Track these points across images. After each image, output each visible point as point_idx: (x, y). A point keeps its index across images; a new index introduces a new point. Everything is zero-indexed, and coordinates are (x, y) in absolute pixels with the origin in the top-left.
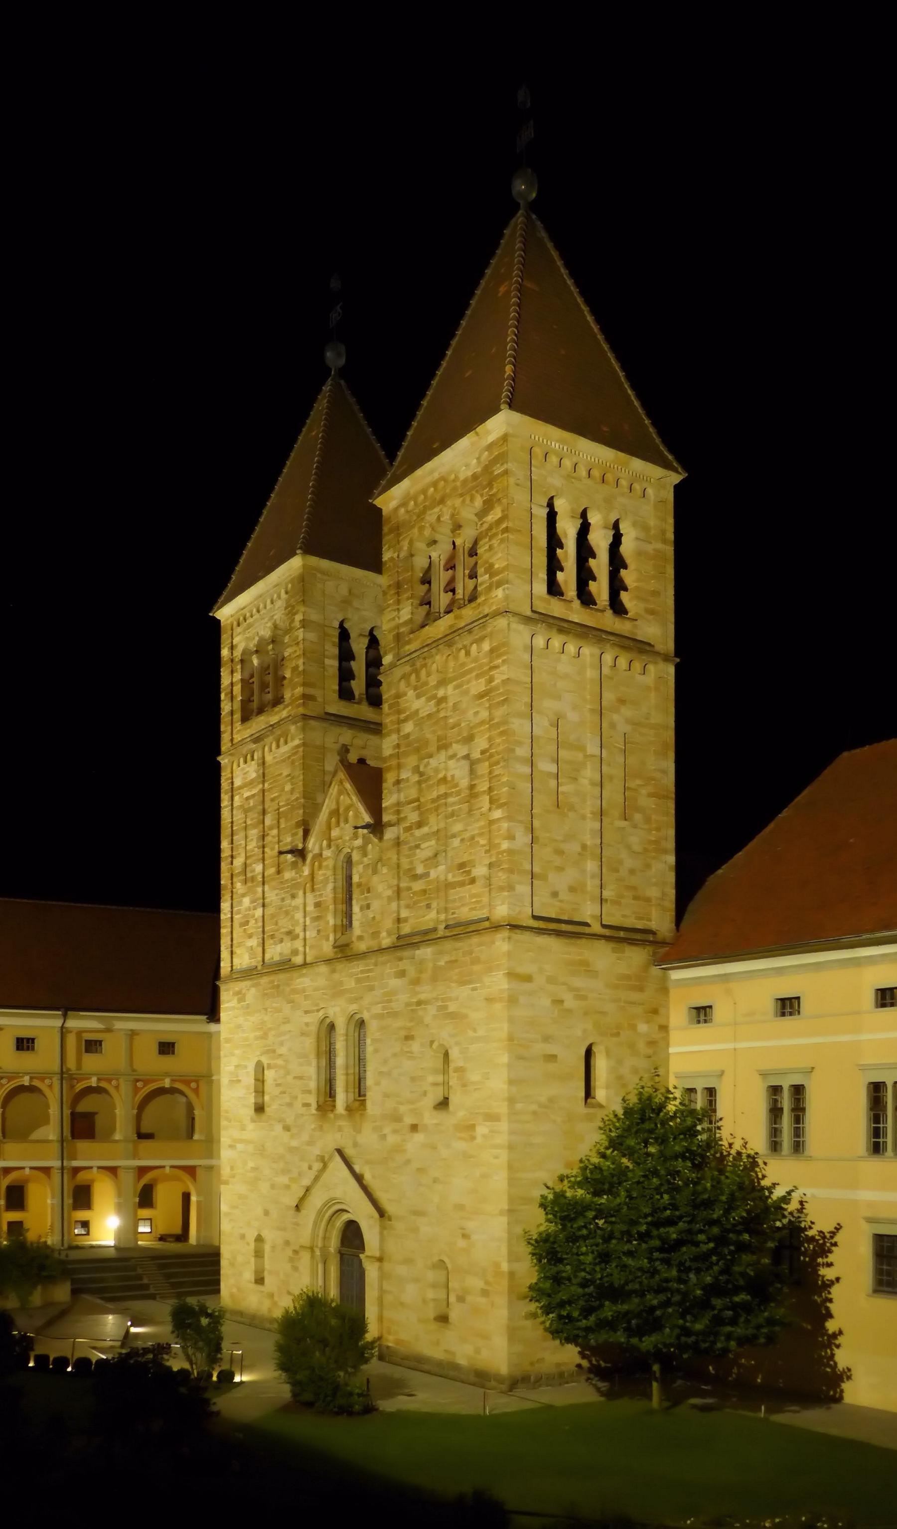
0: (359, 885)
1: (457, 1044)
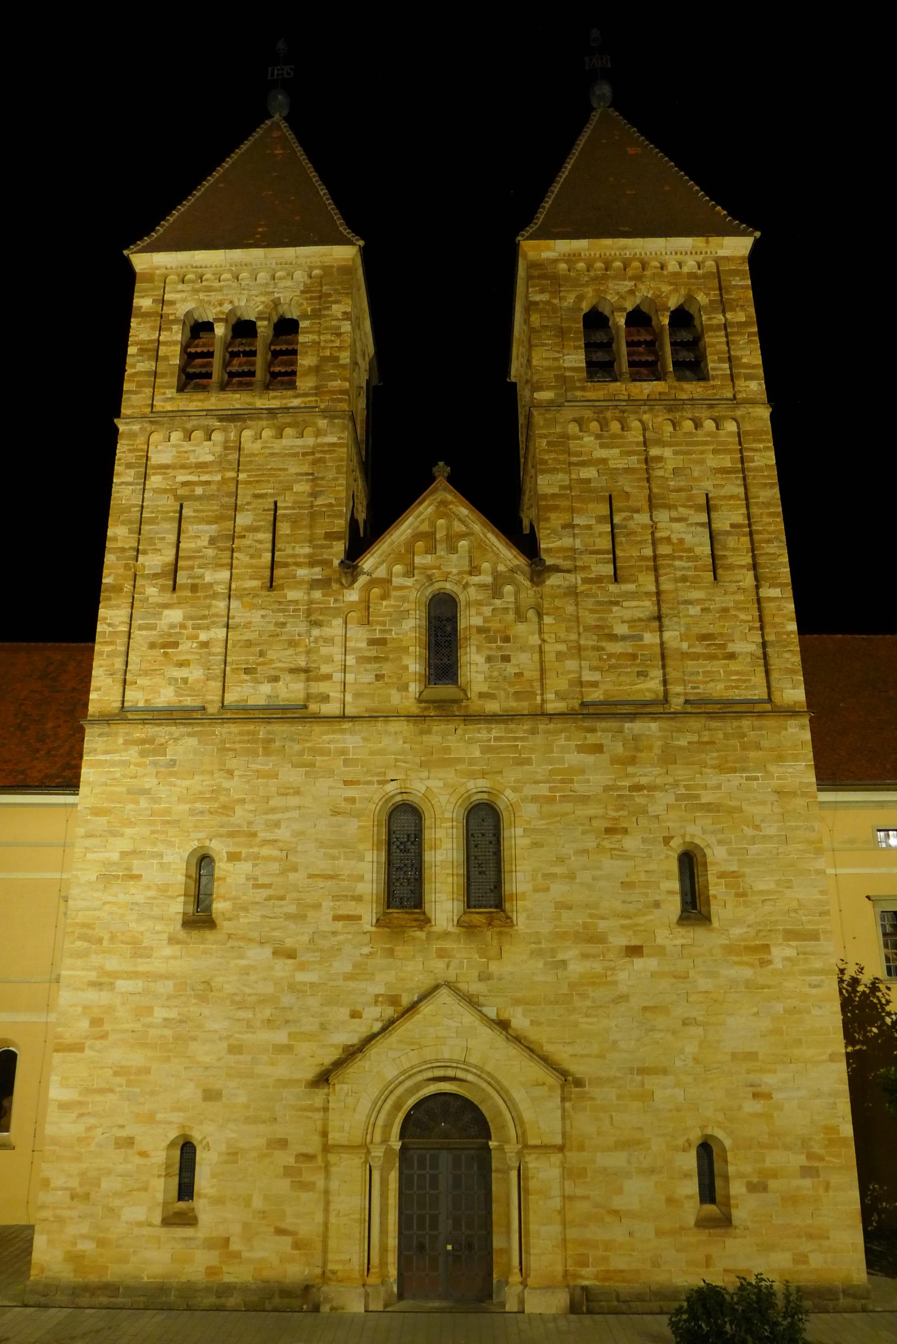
0: (480, 630)
1: (720, 842)
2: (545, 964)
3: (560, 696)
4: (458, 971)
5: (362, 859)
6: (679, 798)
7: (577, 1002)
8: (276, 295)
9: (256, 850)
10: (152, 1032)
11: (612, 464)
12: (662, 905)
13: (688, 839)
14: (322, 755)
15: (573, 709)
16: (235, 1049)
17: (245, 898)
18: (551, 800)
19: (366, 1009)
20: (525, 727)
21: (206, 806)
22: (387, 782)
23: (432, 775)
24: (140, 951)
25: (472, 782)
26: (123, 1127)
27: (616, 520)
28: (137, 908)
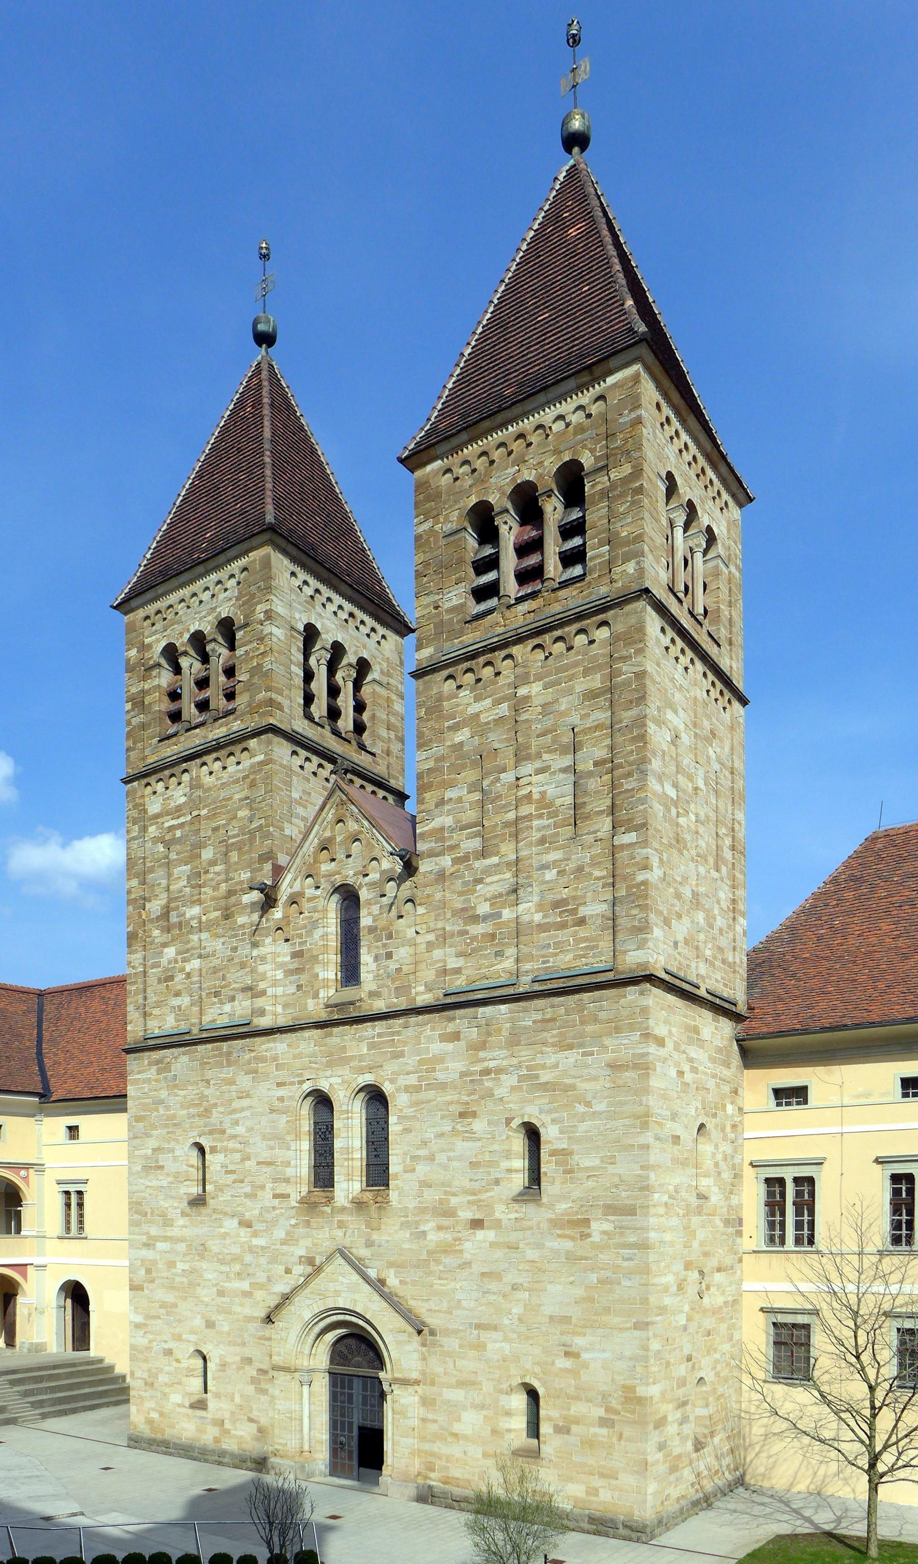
0: (372, 930)
3: (429, 989)
6: (521, 1079)
10: (177, 1279)
12: (501, 1183)
15: (438, 999)
18: (417, 1089)
22: (304, 1081)
26: (166, 1342)
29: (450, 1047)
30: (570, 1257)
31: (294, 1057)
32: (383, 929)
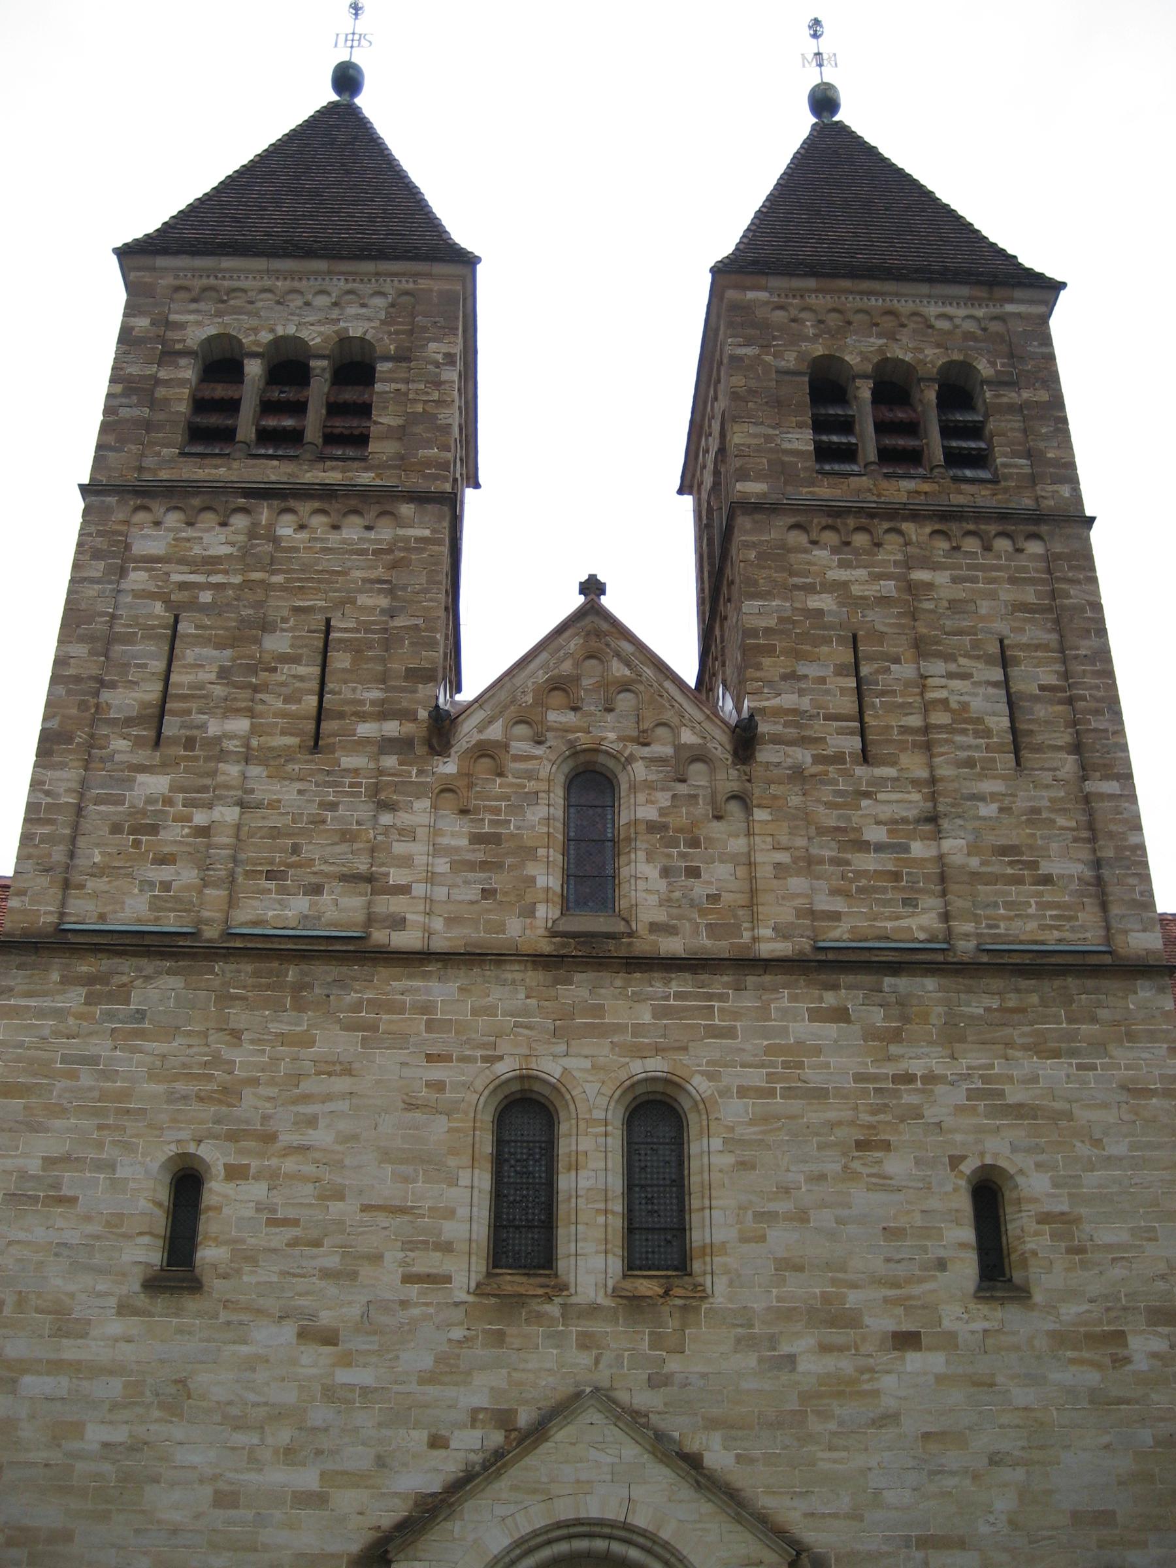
1: (1039, 1166)
2: (761, 1360)
4: (614, 1370)
5: (453, 1182)
6: (972, 1094)
7: (814, 1425)
8: (342, 324)
9: (274, 1162)
10: (80, 1466)
11: (856, 590)
12: (949, 1266)
13: (988, 1161)
14: (390, 1011)
15: (801, 952)
16: (225, 1499)
17: (253, 1241)
19: (456, 1433)
20: (725, 979)
21: (192, 1088)
23: (572, 1051)
24: (65, 1323)
25: (639, 1061)
27: (865, 670)
28: (66, 1252)
29: (832, 1030)
30: (1099, 1399)
31: (475, 1012)
32: (680, 830)
